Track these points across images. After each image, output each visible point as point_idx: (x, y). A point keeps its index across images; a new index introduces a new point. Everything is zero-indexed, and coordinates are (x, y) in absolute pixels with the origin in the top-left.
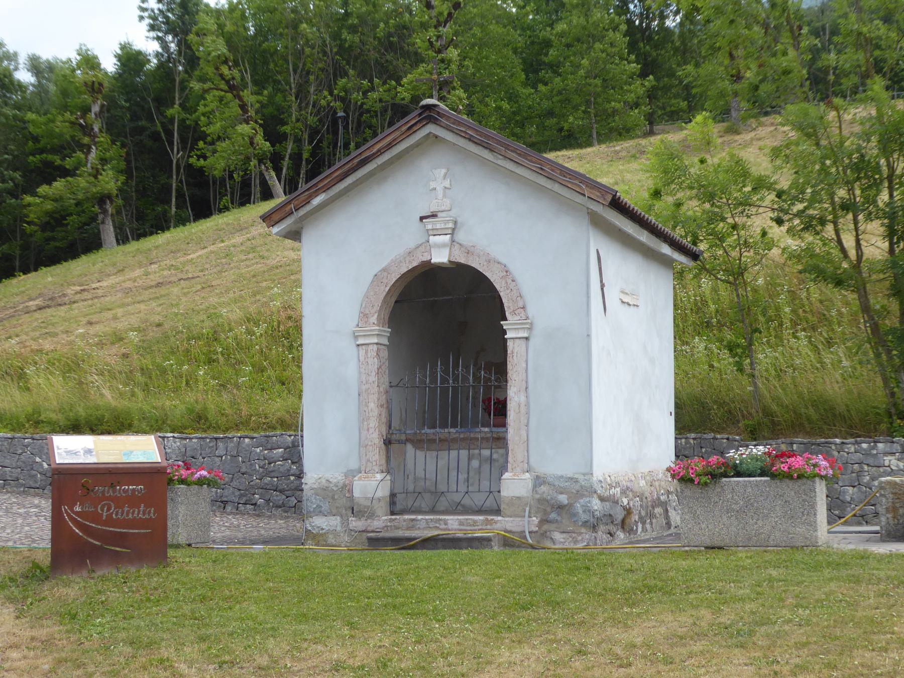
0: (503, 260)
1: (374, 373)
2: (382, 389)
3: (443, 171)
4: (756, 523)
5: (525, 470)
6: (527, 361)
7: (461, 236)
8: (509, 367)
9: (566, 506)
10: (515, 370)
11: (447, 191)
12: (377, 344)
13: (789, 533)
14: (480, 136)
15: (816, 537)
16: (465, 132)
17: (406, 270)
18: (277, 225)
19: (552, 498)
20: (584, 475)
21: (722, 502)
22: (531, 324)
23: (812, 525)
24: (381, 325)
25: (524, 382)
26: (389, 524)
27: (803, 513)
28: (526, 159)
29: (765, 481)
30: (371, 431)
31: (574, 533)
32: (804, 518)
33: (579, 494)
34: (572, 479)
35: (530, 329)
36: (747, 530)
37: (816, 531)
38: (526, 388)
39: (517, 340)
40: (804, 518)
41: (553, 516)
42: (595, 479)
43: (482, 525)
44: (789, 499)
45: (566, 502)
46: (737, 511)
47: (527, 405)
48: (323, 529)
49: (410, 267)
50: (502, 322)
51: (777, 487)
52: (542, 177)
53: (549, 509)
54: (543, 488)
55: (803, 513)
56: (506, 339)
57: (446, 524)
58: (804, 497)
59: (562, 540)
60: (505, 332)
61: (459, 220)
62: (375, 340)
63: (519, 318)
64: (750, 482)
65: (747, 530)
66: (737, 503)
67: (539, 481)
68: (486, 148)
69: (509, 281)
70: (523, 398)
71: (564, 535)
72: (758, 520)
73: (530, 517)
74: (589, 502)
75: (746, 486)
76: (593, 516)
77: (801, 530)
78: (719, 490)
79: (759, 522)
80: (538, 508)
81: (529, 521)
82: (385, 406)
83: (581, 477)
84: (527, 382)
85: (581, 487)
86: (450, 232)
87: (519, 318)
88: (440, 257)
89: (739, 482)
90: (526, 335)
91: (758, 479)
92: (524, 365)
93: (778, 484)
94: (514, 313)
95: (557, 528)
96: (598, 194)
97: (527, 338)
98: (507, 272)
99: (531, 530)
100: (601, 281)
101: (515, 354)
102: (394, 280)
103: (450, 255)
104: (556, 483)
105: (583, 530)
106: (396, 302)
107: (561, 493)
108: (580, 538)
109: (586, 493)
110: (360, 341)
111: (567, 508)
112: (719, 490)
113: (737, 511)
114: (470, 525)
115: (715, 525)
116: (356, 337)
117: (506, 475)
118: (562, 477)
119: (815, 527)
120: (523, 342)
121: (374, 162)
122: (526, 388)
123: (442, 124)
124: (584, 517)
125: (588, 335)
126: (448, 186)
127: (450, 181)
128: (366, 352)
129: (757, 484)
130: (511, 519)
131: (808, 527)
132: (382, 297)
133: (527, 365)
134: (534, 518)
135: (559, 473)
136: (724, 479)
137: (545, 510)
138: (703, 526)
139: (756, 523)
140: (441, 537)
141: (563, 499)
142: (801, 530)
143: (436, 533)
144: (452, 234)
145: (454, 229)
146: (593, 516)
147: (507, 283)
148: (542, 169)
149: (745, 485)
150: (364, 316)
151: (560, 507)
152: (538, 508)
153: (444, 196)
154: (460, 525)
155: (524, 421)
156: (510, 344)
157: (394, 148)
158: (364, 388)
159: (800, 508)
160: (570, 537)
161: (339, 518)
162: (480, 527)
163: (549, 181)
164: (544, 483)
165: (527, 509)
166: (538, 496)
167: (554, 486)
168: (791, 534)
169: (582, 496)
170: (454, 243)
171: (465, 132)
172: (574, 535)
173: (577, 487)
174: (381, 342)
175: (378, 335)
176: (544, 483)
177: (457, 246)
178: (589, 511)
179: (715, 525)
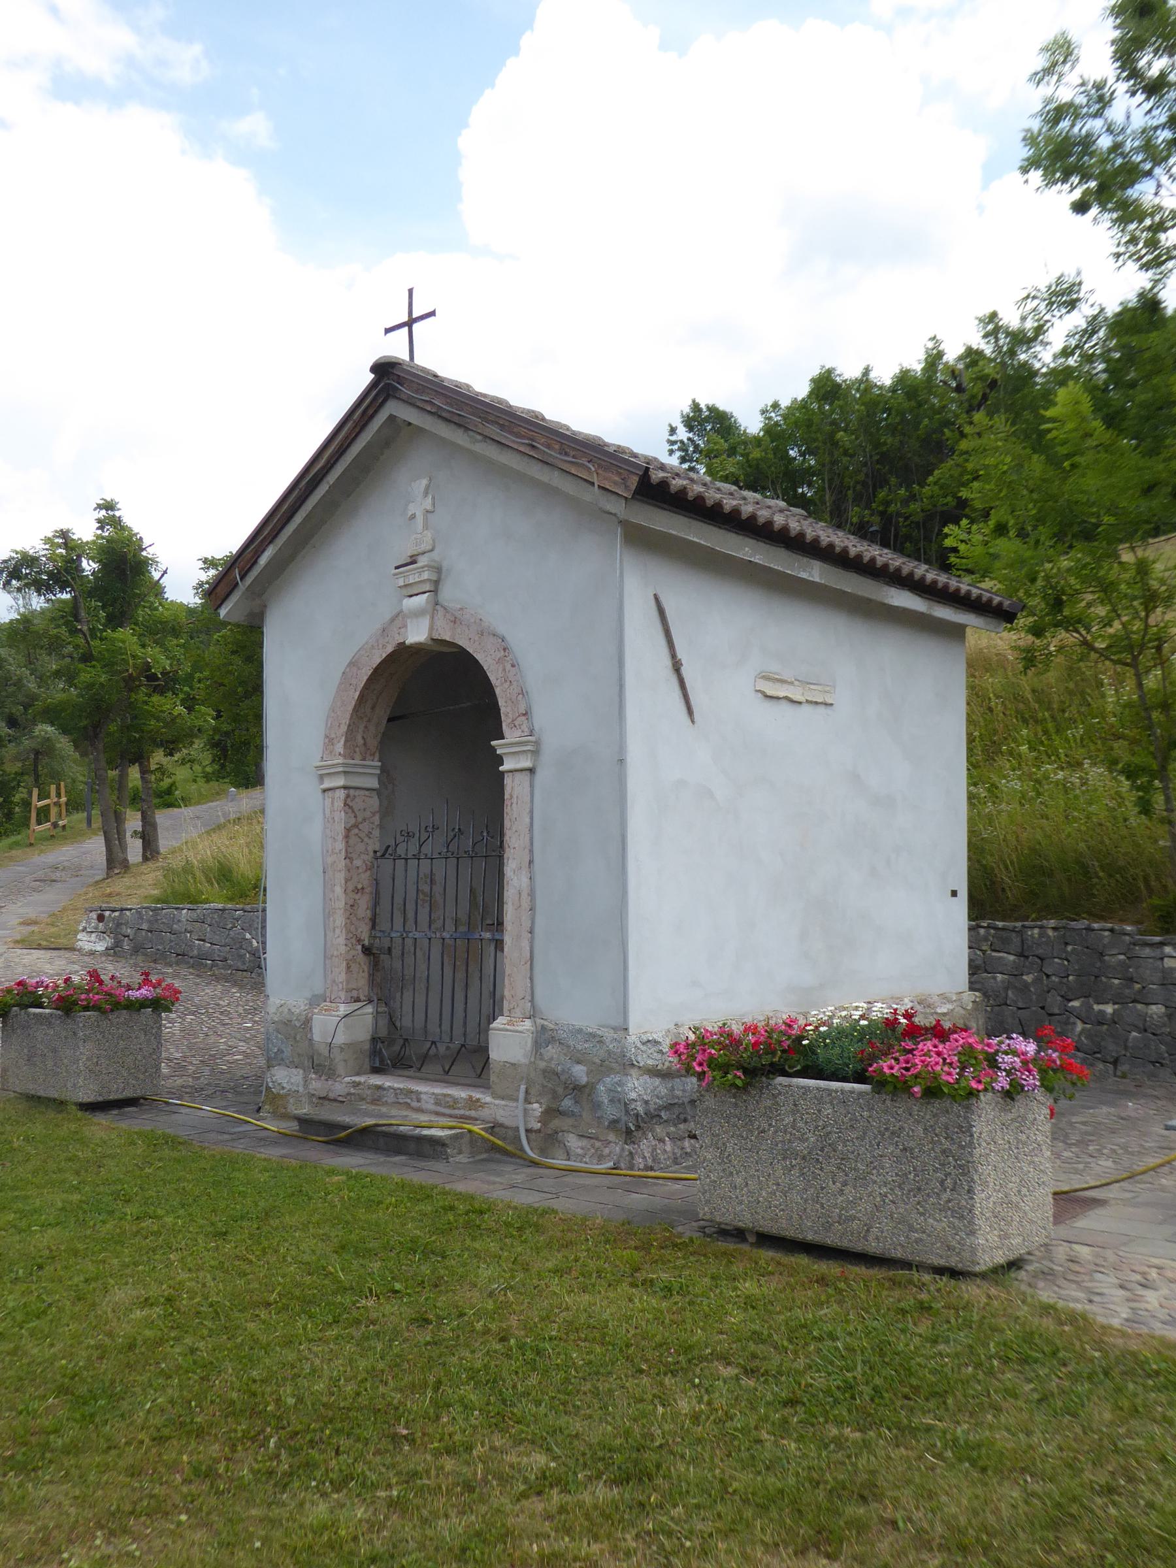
0: (502, 630)
1: (340, 837)
2: (358, 863)
3: (425, 482)
4: (841, 1192)
5: (528, 1015)
6: (531, 812)
7: (448, 593)
8: (507, 823)
9: (584, 1086)
10: (514, 829)
11: (429, 515)
12: (345, 788)
13: (911, 1229)
14: (452, 406)
15: (973, 1251)
16: (430, 402)
17: (379, 661)
18: (224, 606)
19: (563, 1070)
20: (615, 1029)
21: (776, 1132)
22: (537, 743)
23: (962, 1217)
24: (358, 756)
25: (527, 851)
26: (352, 1090)
27: (942, 1183)
28: (511, 433)
29: (861, 1094)
30: (338, 931)
31: (597, 1139)
32: (945, 1196)
33: (602, 1068)
34: (593, 1035)
35: (536, 753)
36: (822, 1207)
37: (972, 1233)
38: (531, 862)
39: (518, 775)
40: (945, 1196)
41: (567, 1103)
42: (632, 1038)
43: (464, 1108)
44: (912, 1144)
45: (584, 1080)
46: (804, 1158)
47: (532, 894)
48: (283, 1088)
49: (384, 656)
50: (493, 743)
51: (886, 1112)
52: (534, 462)
53: (560, 1090)
54: (551, 1051)
55: (942, 1183)
56: (503, 773)
57: (419, 1100)
58: (947, 1144)
59: (579, 1151)
60: (500, 760)
61: (445, 565)
62: (341, 781)
63: (519, 733)
64: (829, 1092)
65: (822, 1207)
66: (803, 1140)
67: (544, 1037)
68: (459, 425)
69: (508, 667)
70: (525, 880)
71: (584, 1142)
72: (845, 1184)
73: (527, 1101)
74: (620, 1084)
75: (820, 1101)
76: (627, 1112)
77: (939, 1224)
78: (769, 1103)
79: (847, 1189)
80: (544, 1086)
81: (525, 1110)
82: (368, 890)
83: (608, 1034)
84: (531, 851)
85: (609, 1052)
86: (427, 587)
87: (519, 733)
88: (417, 634)
89: (807, 1089)
90: (526, 763)
91: (848, 1086)
92: (527, 820)
93: (888, 1103)
94: (513, 725)
95: (574, 1126)
96: (617, 479)
97: (531, 771)
98: (504, 650)
99: (530, 1127)
100: (673, 655)
101: (514, 800)
102: (365, 678)
103: (431, 628)
104: (571, 1043)
105: (611, 1137)
106: (389, 720)
107: (578, 1063)
108: (606, 1151)
109: (614, 1065)
110: (326, 785)
111: (587, 1090)
112: (769, 1103)
113: (804, 1158)
114: (449, 1107)
115: (760, 1182)
116: (321, 778)
117: (500, 1022)
118: (580, 1031)
119: (971, 1223)
120: (525, 777)
121: (325, 481)
122: (531, 862)
123: (403, 396)
124: (611, 1112)
125: (621, 761)
126: (429, 507)
127: (433, 498)
128: (333, 799)
129: (844, 1099)
130: (503, 1103)
131: (956, 1221)
132: (350, 708)
133: (532, 818)
134: (536, 1106)
135: (578, 1023)
136: (781, 1080)
137: (554, 1092)
138: (739, 1181)
139: (841, 1192)
140: (380, 1129)
141: (580, 1073)
142: (939, 1224)
143: (370, 1121)
144: (435, 591)
145: (437, 583)
146: (627, 1112)
147: (504, 670)
148: (533, 446)
149: (821, 1097)
150: (330, 741)
151: (577, 1090)
152: (544, 1086)
153: (426, 526)
154: (436, 1104)
155: (527, 924)
156: (508, 780)
157: (348, 452)
158: (330, 860)
159: (936, 1170)
160: (593, 1146)
161: (301, 1071)
162: (462, 1112)
163: (546, 469)
164: (552, 1040)
165: (523, 1088)
166: (542, 1065)
167: (569, 1047)
168: (916, 1231)
169: (610, 1071)
170: (438, 607)
171: (430, 402)
172: (598, 1144)
173: (602, 1053)
174: (353, 784)
175: (345, 772)
176: (552, 1040)
177: (441, 612)
178: (619, 1101)
179: (760, 1182)
